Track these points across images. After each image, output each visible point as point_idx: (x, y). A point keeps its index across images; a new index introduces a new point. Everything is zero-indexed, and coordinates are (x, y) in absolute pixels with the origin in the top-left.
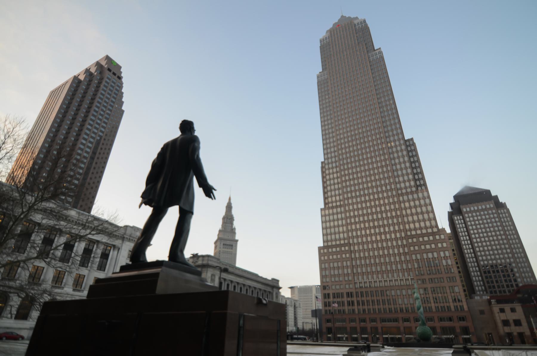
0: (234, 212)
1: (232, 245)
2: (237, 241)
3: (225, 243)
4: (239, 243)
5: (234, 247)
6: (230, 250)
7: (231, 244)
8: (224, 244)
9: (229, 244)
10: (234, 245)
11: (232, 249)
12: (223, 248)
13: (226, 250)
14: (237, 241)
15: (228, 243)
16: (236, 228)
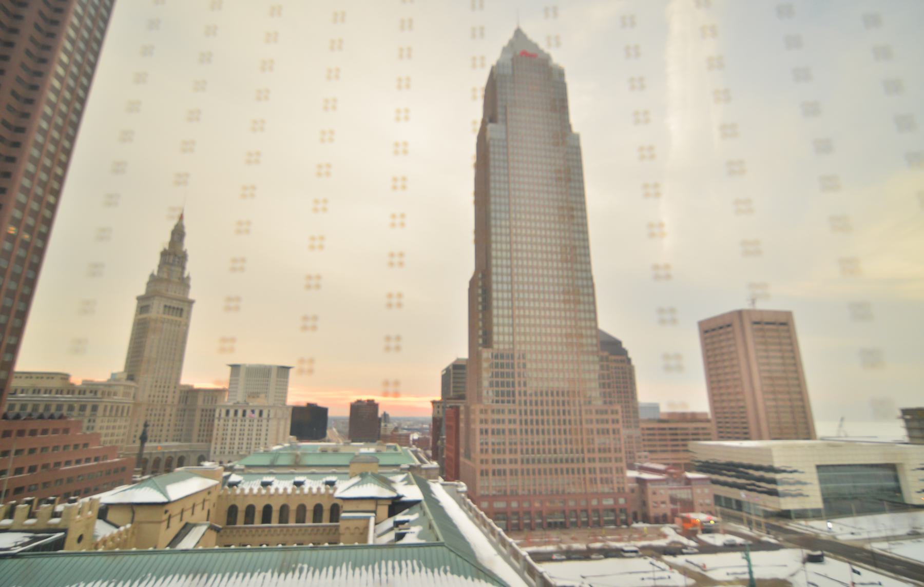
0: (189, 244)
1: (182, 310)
2: (191, 302)
3: (168, 304)
4: (195, 306)
5: (185, 314)
6: (178, 319)
7: (180, 307)
8: (165, 306)
9: (176, 306)
10: (185, 309)
11: (181, 315)
12: (164, 313)
13: (171, 317)
14: (191, 302)
15: (175, 304)
16: (192, 276)
